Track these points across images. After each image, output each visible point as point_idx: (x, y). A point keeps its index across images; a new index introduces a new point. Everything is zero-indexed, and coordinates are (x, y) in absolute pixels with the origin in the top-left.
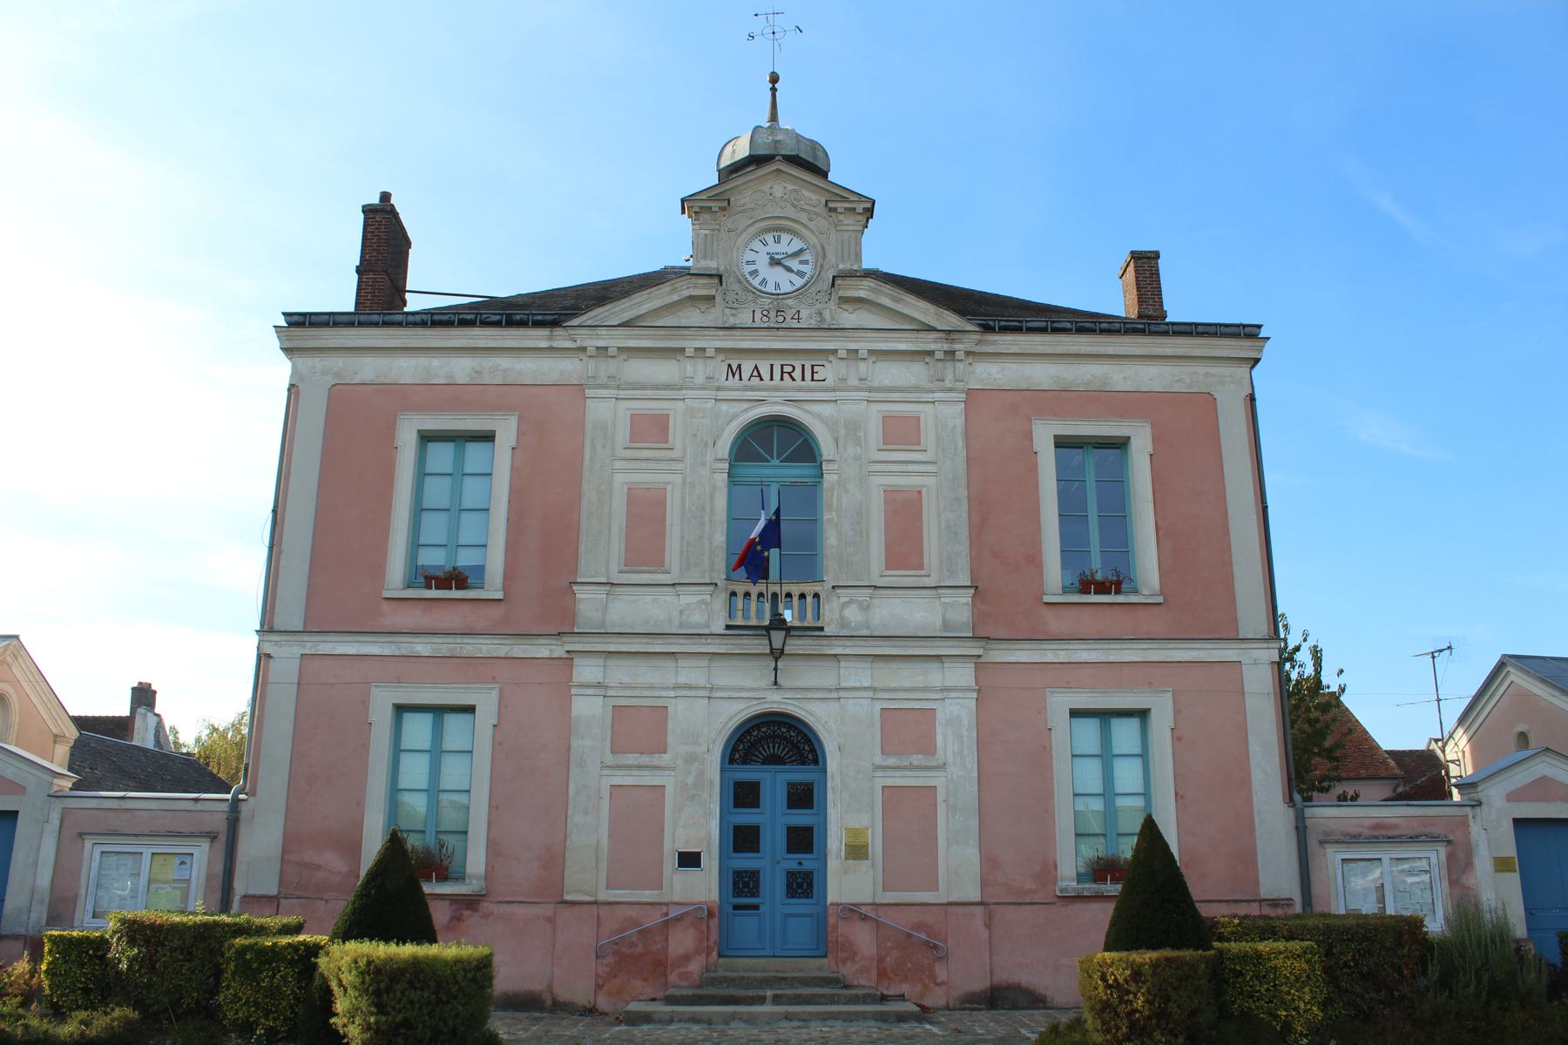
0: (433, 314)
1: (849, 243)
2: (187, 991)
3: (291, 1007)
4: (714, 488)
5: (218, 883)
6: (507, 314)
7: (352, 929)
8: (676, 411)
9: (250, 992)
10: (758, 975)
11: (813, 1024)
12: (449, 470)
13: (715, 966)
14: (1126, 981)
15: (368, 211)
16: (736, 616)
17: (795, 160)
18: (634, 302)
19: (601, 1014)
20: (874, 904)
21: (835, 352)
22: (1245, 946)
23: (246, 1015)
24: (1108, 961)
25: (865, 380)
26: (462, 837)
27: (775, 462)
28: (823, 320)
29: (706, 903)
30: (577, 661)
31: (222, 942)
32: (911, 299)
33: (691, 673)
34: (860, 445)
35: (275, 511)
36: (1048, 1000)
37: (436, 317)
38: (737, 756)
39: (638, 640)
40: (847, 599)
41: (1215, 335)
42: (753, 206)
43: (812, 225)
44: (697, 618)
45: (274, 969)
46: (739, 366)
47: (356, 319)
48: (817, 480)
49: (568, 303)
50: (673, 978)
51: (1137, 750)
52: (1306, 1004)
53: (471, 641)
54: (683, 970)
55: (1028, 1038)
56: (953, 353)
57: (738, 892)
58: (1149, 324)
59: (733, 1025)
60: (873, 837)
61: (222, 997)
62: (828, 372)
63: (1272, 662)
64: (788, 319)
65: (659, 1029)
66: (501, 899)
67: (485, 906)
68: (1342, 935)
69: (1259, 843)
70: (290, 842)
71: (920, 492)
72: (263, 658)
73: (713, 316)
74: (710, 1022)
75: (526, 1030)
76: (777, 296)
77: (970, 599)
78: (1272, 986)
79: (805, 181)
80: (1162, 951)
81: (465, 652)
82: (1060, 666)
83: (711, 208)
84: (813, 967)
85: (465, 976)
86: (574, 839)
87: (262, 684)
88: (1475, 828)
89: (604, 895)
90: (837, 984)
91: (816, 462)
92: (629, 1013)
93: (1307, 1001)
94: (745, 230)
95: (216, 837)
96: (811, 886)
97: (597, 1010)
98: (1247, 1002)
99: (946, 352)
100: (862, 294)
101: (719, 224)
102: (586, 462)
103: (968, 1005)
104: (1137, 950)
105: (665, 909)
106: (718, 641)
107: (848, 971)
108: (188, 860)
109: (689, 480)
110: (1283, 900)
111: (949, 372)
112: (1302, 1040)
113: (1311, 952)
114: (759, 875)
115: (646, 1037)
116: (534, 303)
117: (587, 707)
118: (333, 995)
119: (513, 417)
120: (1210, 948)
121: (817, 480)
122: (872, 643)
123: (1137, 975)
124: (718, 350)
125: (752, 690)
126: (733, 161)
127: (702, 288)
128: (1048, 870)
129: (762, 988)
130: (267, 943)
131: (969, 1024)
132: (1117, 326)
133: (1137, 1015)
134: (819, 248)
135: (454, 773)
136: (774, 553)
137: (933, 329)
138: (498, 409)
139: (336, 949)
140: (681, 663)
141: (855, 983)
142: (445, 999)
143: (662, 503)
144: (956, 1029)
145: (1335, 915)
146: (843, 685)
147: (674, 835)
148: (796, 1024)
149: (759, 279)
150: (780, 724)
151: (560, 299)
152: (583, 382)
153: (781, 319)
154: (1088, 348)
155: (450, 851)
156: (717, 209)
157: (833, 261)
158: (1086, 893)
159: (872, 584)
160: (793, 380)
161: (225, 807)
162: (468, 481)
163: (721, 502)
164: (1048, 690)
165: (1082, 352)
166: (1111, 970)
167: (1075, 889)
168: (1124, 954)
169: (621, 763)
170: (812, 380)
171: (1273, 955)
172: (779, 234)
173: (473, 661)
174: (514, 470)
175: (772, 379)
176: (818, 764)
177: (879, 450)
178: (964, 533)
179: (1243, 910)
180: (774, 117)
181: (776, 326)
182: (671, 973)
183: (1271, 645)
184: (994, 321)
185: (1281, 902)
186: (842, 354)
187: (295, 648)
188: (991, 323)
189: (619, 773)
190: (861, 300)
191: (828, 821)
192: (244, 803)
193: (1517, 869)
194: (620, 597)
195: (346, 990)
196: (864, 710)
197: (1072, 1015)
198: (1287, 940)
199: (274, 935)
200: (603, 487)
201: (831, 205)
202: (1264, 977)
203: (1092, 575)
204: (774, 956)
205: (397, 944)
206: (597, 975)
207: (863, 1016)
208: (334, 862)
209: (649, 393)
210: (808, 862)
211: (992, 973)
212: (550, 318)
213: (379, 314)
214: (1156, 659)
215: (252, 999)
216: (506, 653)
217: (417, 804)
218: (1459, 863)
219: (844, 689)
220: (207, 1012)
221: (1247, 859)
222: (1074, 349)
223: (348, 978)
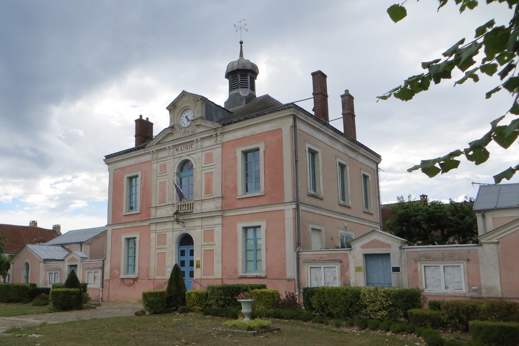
33: (169, 226)
64: (187, 133)
67: (138, 280)
88: (350, 257)
117: (153, 236)
128: (236, 271)
183: (292, 204)
193: (363, 271)
218: (344, 270)
222: (245, 125)
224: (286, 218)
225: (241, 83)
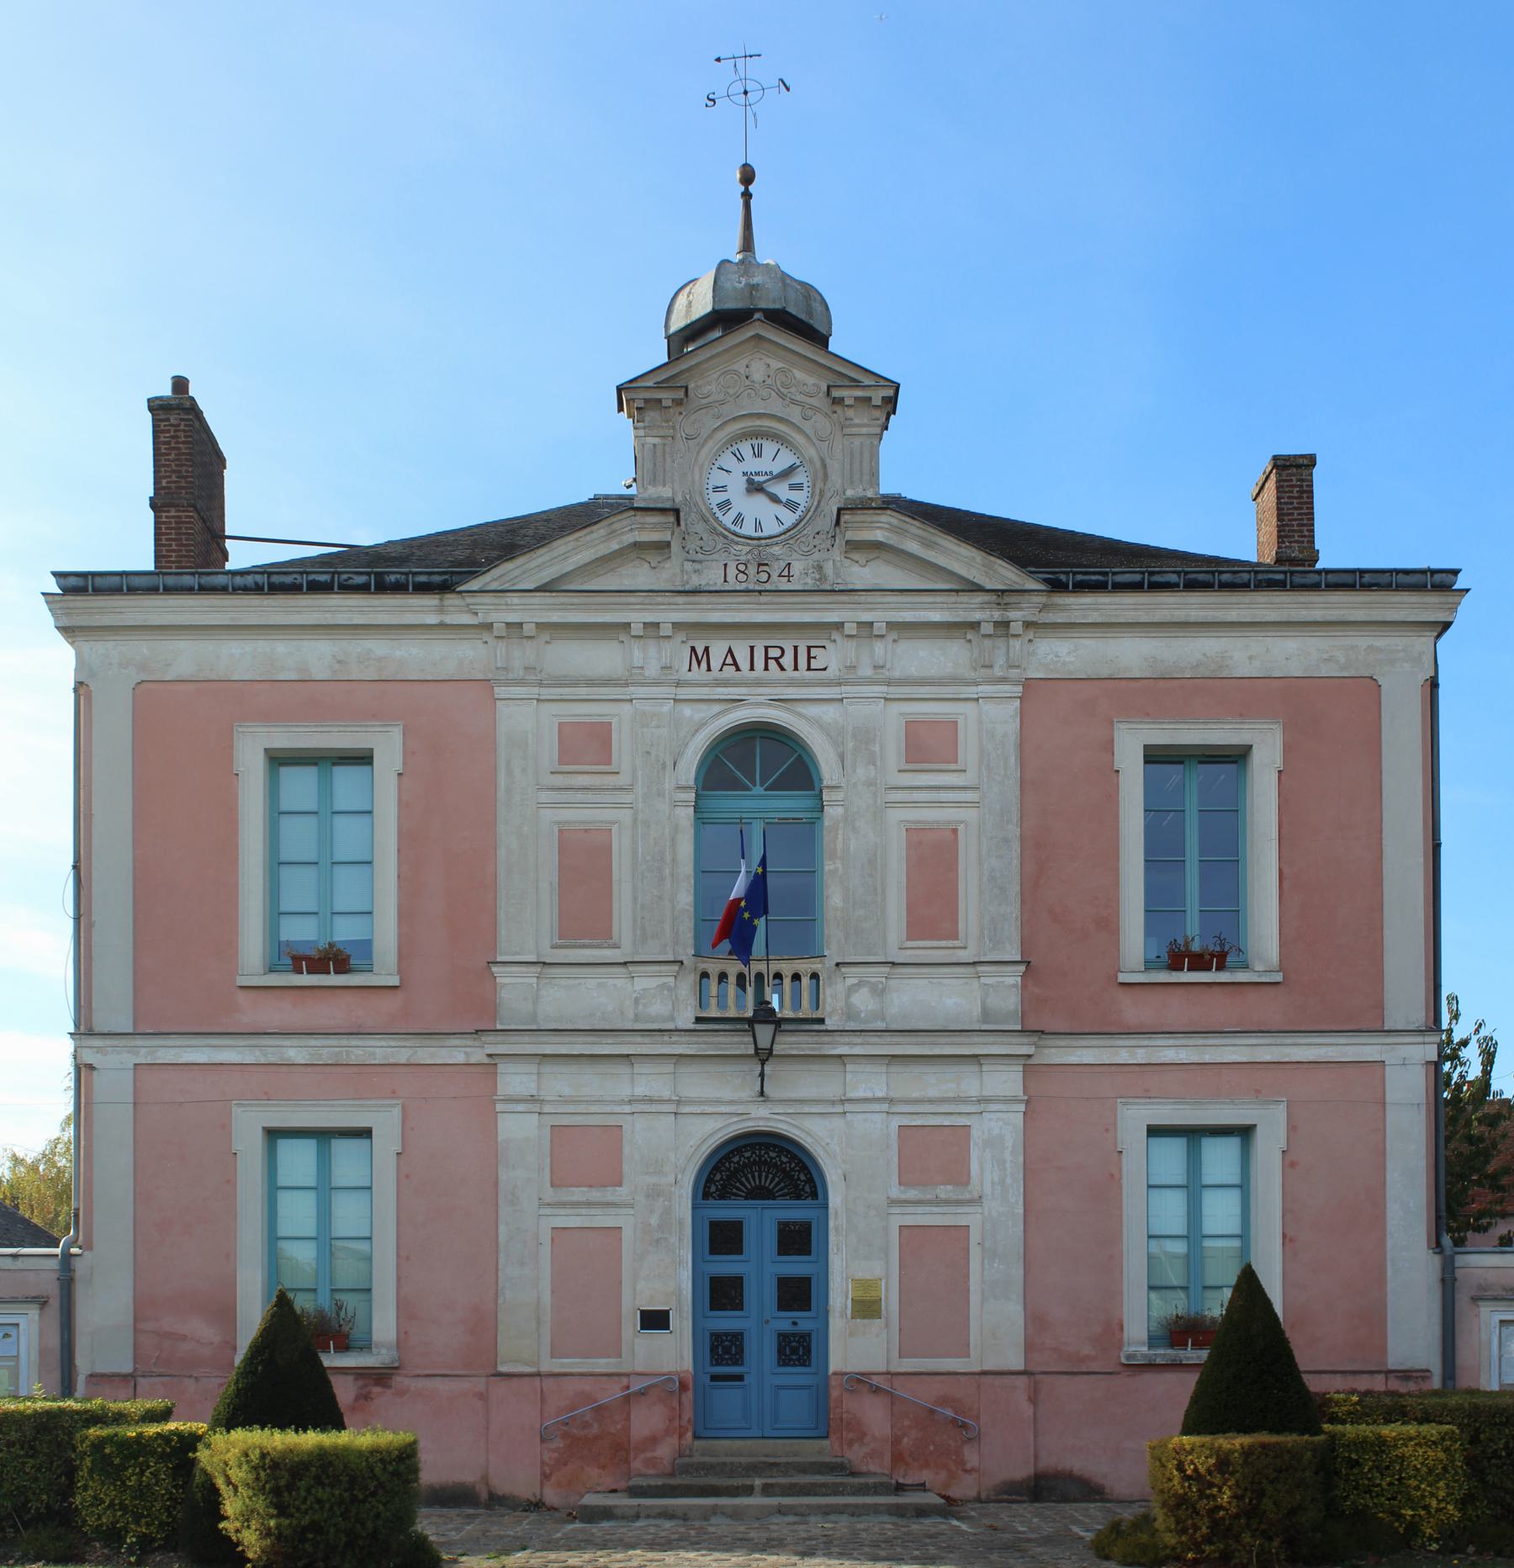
0: (270, 574)
1: (861, 454)
2: (34, 1493)
3: (168, 1510)
7: (237, 1415)
8: (621, 717)
9: (114, 1493)
10: (743, 1460)
11: (812, 1519)
12: (312, 807)
13: (691, 1450)
14: (1209, 1472)
15: (157, 407)
16: (708, 1005)
17: (781, 319)
18: (555, 553)
19: (549, 1510)
20: (888, 1373)
21: (839, 626)
22: (1365, 1430)
23: (111, 1519)
24: (1188, 1447)
25: (882, 667)
26: (363, 1296)
27: (758, 790)
28: (823, 578)
29: (677, 1373)
30: (501, 1068)
31: (70, 1433)
32: (949, 543)
33: (651, 1082)
34: (874, 764)
35: (76, 867)
36: (1106, 1491)
37: (276, 579)
38: (713, 1189)
39: (580, 1039)
40: (855, 981)
41: (1387, 587)
42: (721, 396)
43: (807, 426)
44: (658, 1010)
45: (141, 1465)
46: (707, 649)
47: (160, 581)
48: (815, 815)
49: (460, 554)
50: (637, 1464)
51: (1236, 1180)
52: (1439, 1501)
53: (359, 1043)
54: (649, 1455)
55: (1081, 1538)
57: (717, 1360)
58: (1292, 573)
59: (713, 1520)
61: (78, 1499)
62: (831, 657)
63: (1428, 1063)
65: (624, 1527)
66: (419, 1372)
67: (399, 1381)
68: (1494, 1417)
70: (143, 1307)
71: (955, 831)
72: (83, 1071)
73: (669, 573)
74: (685, 1518)
75: (458, 1530)
76: (758, 541)
77: (1019, 979)
78: (1398, 1480)
79: (797, 354)
80: (1256, 1435)
81: (353, 1057)
82: (1137, 1068)
83: (660, 401)
84: (812, 1450)
85: (384, 1469)
87: (85, 1103)
89: (548, 1365)
91: (813, 789)
92: (585, 1507)
93: (1440, 1498)
94: (710, 437)
95: (46, 1302)
96: (808, 1350)
97: (544, 1504)
98: (1363, 1498)
99: (997, 624)
100: (879, 535)
102: (501, 794)
103: (1005, 1497)
104: (1224, 1432)
105: (625, 1381)
106: (685, 1039)
107: (855, 1455)
109: (641, 817)
112: (1430, 1545)
113: (1451, 1439)
114: (742, 1339)
115: (608, 1537)
116: (413, 554)
118: (220, 1495)
119: (396, 729)
120: (1320, 1431)
121: (815, 815)
122: (889, 1039)
123: (1223, 1463)
125: (732, 1102)
126: (689, 322)
127: (651, 530)
128: (1113, 1330)
130: (129, 1434)
131: (1007, 1519)
132: (1246, 577)
133: (1222, 1513)
134: (818, 464)
135: (348, 1215)
136: (760, 923)
137: (978, 589)
139: (219, 1439)
140: (638, 1068)
141: (864, 1469)
142: (361, 1496)
143: (606, 851)
144: (991, 1526)
145: (1487, 1392)
146: (850, 1095)
147: (635, 1290)
148: (791, 1518)
149: (732, 515)
150: (768, 1146)
151: (449, 548)
152: (490, 676)
153: (764, 577)
155: (350, 1314)
156: (669, 403)
157: (838, 486)
158: (1159, 1361)
159: (890, 960)
160: (782, 669)
161: (54, 1264)
162: (341, 822)
164: (1119, 1100)
165: (1192, 620)
166: (1190, 1457)
167: (1144, 1356)
168: (1207, 1439)
170: (809, 669)
171: (1401, 1442)
172: (760, 441)
174: (403, 805)
175: (752, 669)
176: (817, 1199)
177: (899, 771)
178: (1015, 888)
179: (1363, 1384)
180: (748, 244)
181: (757, 588)
182: (635, 1458)
183: (1427, 1039)
184: (1067, 573)
185: (1414, 1374)
186: (850, 629)
188: (1063, 577)
189: (562, 1212)
190: (877, 546)
191: (830, 1270)
192: (77, 1258)
195: (236, 1489)
196: (877, 1127)
197: (1138, 1510)
198: (1420, 1423)
199: (137, 1423)
201: (836, 393)
202: (1387, 1468)
203: (1187, 944)
204: (763, 1437)
205: (297, 1431)
206: (543, 1463)
207: (875, 1510)
208: (203, 1331)
209: (583, 692)
210: (804, 1322)
211: (1036, 1457)
212: (437, 579)
213: (193, 574)
214: (1268, 1058)
215: (117, 1502)
216: (408, 1059)
217: (303, 1255)
219: (850, 1100)
220: (63, 1517)
221: (1373, 1319)
222: (1180, 615)
223: (238, 1474)
224: (1390, 1097)
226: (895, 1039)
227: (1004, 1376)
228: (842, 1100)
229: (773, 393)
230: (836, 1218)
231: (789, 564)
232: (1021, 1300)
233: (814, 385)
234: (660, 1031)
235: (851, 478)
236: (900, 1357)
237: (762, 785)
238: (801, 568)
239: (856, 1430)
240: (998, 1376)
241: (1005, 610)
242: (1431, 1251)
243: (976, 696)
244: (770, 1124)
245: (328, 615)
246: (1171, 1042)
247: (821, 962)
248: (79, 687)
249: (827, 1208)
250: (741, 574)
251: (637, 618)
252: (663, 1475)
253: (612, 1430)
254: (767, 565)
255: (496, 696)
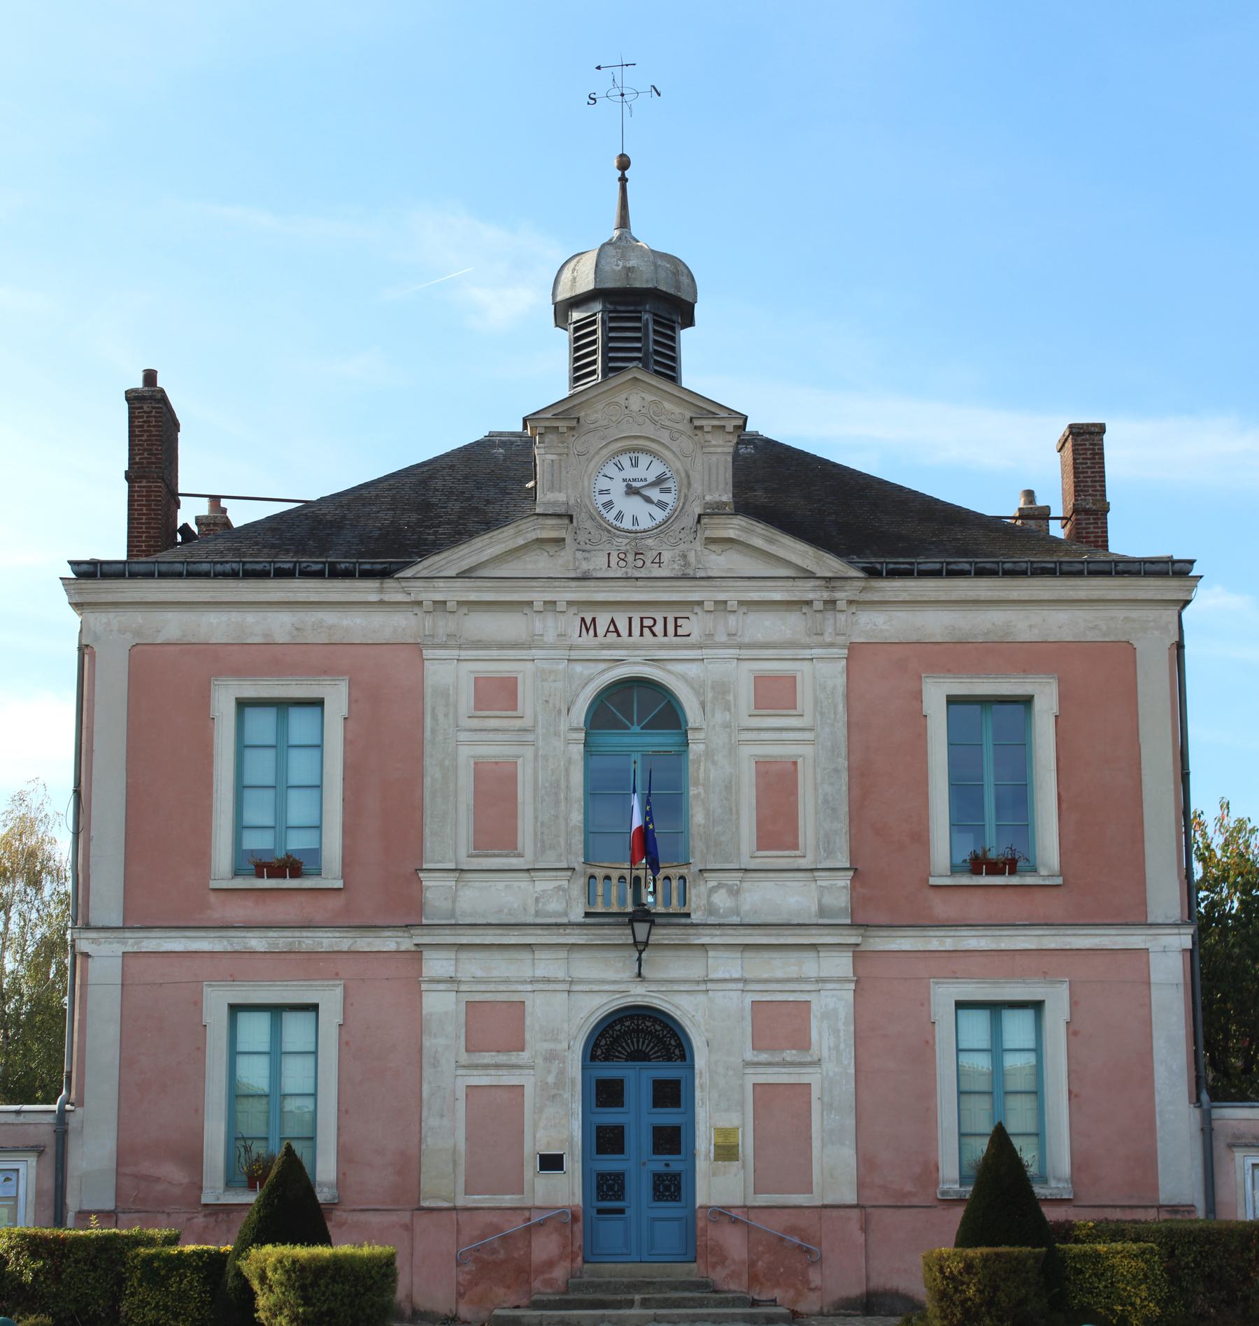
4: (569, 761)
5: (49, 1199)
6: (329, 563)
8: (524, 672)
10: (624, 1280)
13: (581, 1273)
16: (595, 904)
20: (745, 1207)
21: (700, 603)
25: (735, 635)
27: (636, 729)
28: (687, 564)
29: (569, 1207)
30: (427, 954)
33: (549, 966)
34: (729, 710)
35: (77, 792)
38: (599, 1052)
39: (491, 932)
40: (715, 884)
42: (606, 423)
44: (555, 905)
46: (594, 620)
48: (682, 748)
50: (536, 1284)
51: (1031, 1045)
53: (309, 934)
54: (547, 1276)
56: (834, 602)
57: (602, 1196)
58: (1061, 563)
60: (743, 1137)
62: (694, 626)
63: (1184, 950)
64: (648, 563)
66: (355, 1207)
69: (1159, 1145)
70: (125, 1154)
71: (795, 763)
77: (849, 882)
81: (304, 946)
82: (947, 954)
84: (681, 1271)
86: (430, 1142)
87: (81, 986)
89: (462, 1201)
90: (706, 1288)
94: (597, 453)
95: (43, 1150)
96: (678, 1188)
97: (459, 1318)
99: (825, 602)
100: (731, 534)
101: (568, 447)
102: (428, 734)
103: (842, 1311)
105: (527, 1214)
106: (577, 931)
107: (718, 1276)
108: (13, 1176)
109: (540, 752)
110: (1183, 1206)
111: (831, 624)
114: (624, 1177)
119: (343, 683)
121: (682, 748)
122: (743, 932)
124: (570, 603)
125: (614, 982)
128: (929, 1172)
129: (629, 1293)
134: (683, 475)
135: (296, 1075)
137: (810, 576)
138: (325, 673)
140: (538, 954)
141: (726, 1288)
143: (513, 778)
146: (712, 976)
147: (535, 1137)
149: (614, 512)
150: (644, 1017)
152: (419, 641)
153: (640, 563)
154: (990, 593)
157: (699, 491)
159: (743, 867)
160: (654, 635)
161: (50, 1119)
163: (577, 777)
164: (931, 980)
165: (982, 598)
167: (956, 1192)
169: (476, 1062)
170: (676, 635)
172: (636, 455)
173: (313, 956)
174: (347, 742)
175: (630, 635)
176: (685, 1060)
178: (844, 809)
179: (1140, 1215)
182: (535, 1280)
183: (1182, 931)
185: (1181, 1209)
187: (115, 945)
188: (878, 566)
189: (475, 1072)
190: (730, 540)
191: (696, 1121)
192: (72, 1113)
194: (469, 883)
196: (734, 1002)
200: (447, 762)
201: (697, 423)
203: (985, 853)
206: (458, 1283)
209: (495, 653)
210: (676, 1164)
211: (868, 1278)
212: (378, 567)
214: (1053, 946)
216: (349, 948)
219: (712, 981)
221: (1146, 1162)
222: (972, 595)
224: (1153, 979)
225: (657, 353)
226: (748, 932)
227: (840, 1210)
228: (705, 981)
229: (647, 420)
230: (701, 1077)
231: (660, 553)
232: (854, 1146)
233: (680, 413)
234: (556, 925)
235: (710, 484)
236: (755, 1193)
237: (638, 725)
238: (670, 557)
239: (719, 1256)
240: (835, 1210)
241: (832, 591)
242: (1192, 1105)
243: (810, 657)
244: (646, 1000)
245: (290, 594)
246: (973, 933)
247: (687, 868)
248: (83, 649)
249: (694, 1068)
250: (621, 562)
251: (538, 597)
252: (558, 1293)
253: (516, 1255)
254: (642, 554)
255: (424, 657)
